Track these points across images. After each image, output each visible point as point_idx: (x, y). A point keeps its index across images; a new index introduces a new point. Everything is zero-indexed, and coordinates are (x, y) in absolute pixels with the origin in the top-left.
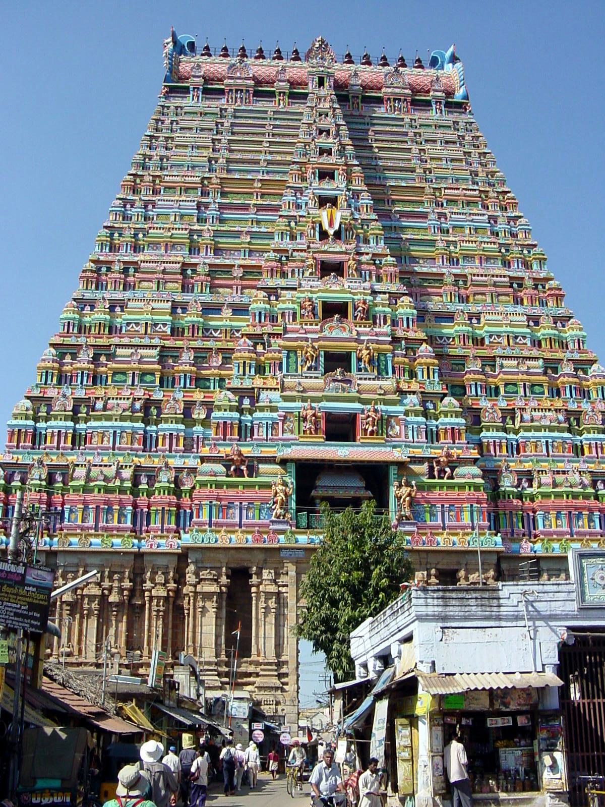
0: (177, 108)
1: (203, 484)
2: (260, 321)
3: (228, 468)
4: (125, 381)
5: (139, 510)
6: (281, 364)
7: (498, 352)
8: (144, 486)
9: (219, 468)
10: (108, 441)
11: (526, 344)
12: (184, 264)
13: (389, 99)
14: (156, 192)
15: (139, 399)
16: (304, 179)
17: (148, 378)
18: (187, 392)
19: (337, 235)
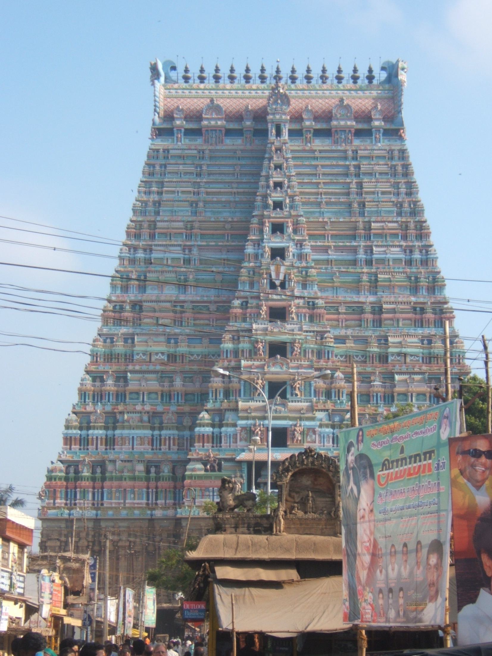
0: (164, 150)
1: (191, 477)
2: (227, 357)
3: (205, 465)
4: (138, 399)
5: (150, 490)
6: (240, 390)
7: (397, 368)
8: (153, 475)
9: (200, 466)
10: (129, 443)
11: (419, 361)
12: (175, 302)
13: (336, 131)
14: (152, 236)
15: (148, 413)
16: (261, 232)
17: (153, 396)
18: (179, 406)
19: (283, 285)
